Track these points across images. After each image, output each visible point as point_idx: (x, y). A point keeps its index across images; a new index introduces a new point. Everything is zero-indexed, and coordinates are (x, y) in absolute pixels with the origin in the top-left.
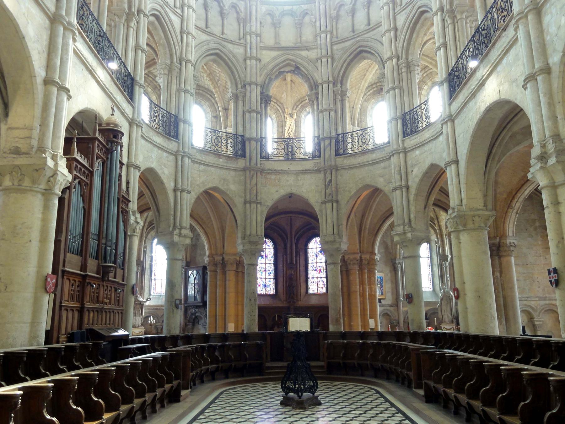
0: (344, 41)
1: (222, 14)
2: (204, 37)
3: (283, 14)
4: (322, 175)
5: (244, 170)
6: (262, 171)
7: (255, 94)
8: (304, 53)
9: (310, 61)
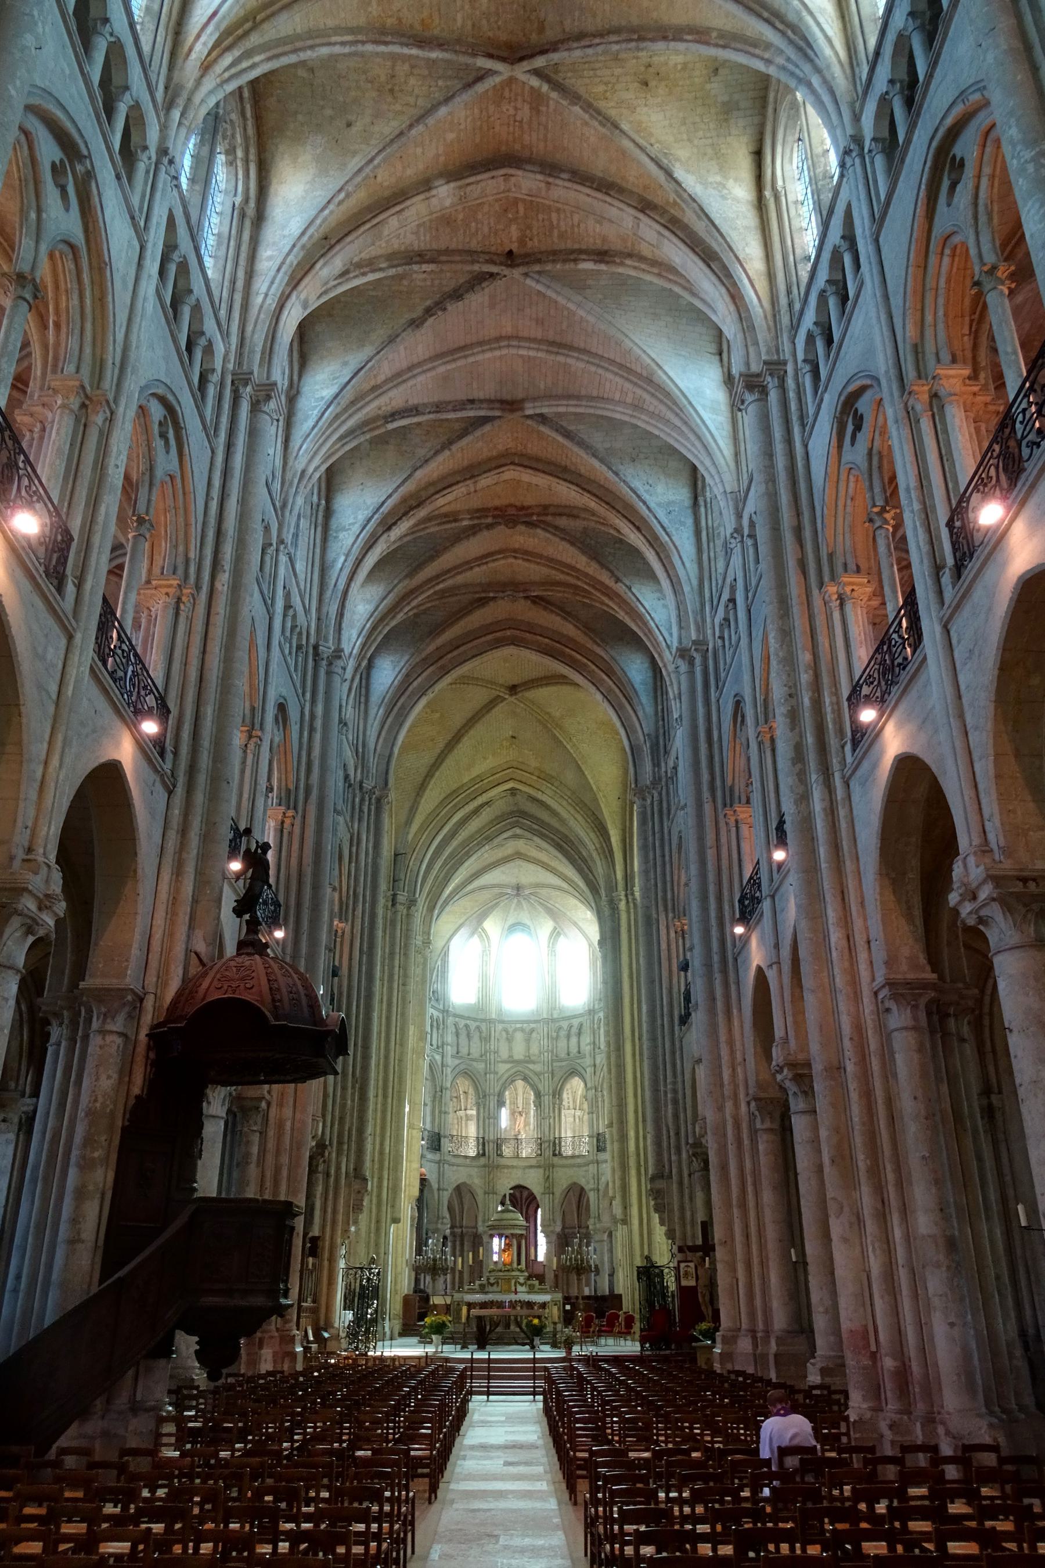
0: (561, 1060)
1: (468, 1036)
2: (457, 1062)
3: (516, 1030)
4: (541, 1171)
5: (484, 1166)
6: (498, 1167)
7: (493, 1102)
8: (531, 1066)
9: (536, 1074)
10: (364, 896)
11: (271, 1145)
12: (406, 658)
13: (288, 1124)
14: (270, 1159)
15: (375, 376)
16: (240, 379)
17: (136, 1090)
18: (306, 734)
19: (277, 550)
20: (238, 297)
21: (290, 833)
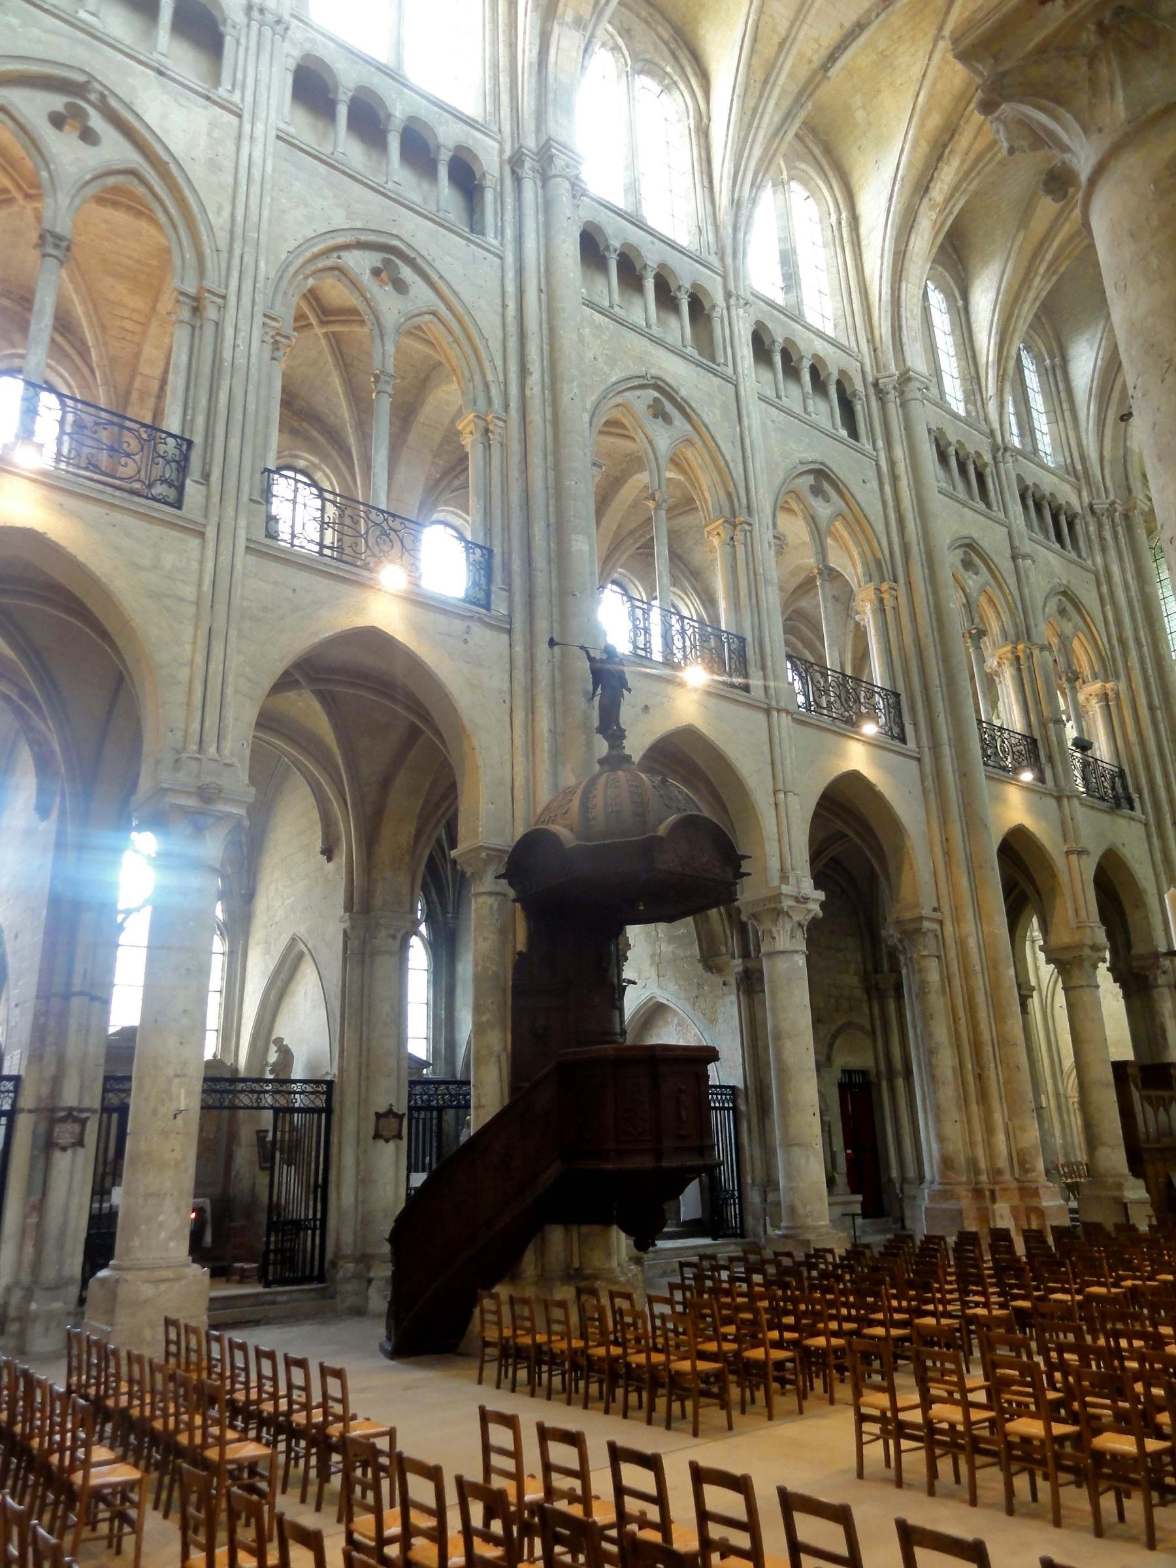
10: (1137, 639)
11: (954, 967)
12: (1101, 327)
13: (972, 942)
14: (957, 982)
15: (774, 30)
16: (515, 162)
17: (521, 946)
18: (887, 488)
19: (728, 308)
20: (504, 79)
21: (895, 609)
